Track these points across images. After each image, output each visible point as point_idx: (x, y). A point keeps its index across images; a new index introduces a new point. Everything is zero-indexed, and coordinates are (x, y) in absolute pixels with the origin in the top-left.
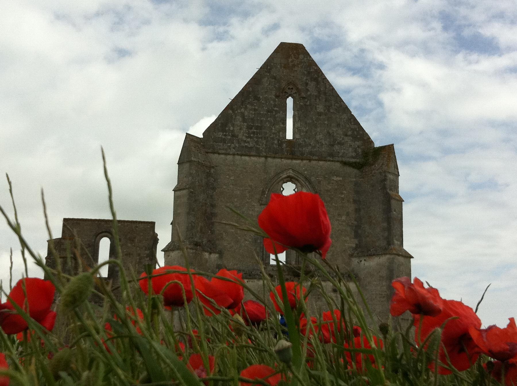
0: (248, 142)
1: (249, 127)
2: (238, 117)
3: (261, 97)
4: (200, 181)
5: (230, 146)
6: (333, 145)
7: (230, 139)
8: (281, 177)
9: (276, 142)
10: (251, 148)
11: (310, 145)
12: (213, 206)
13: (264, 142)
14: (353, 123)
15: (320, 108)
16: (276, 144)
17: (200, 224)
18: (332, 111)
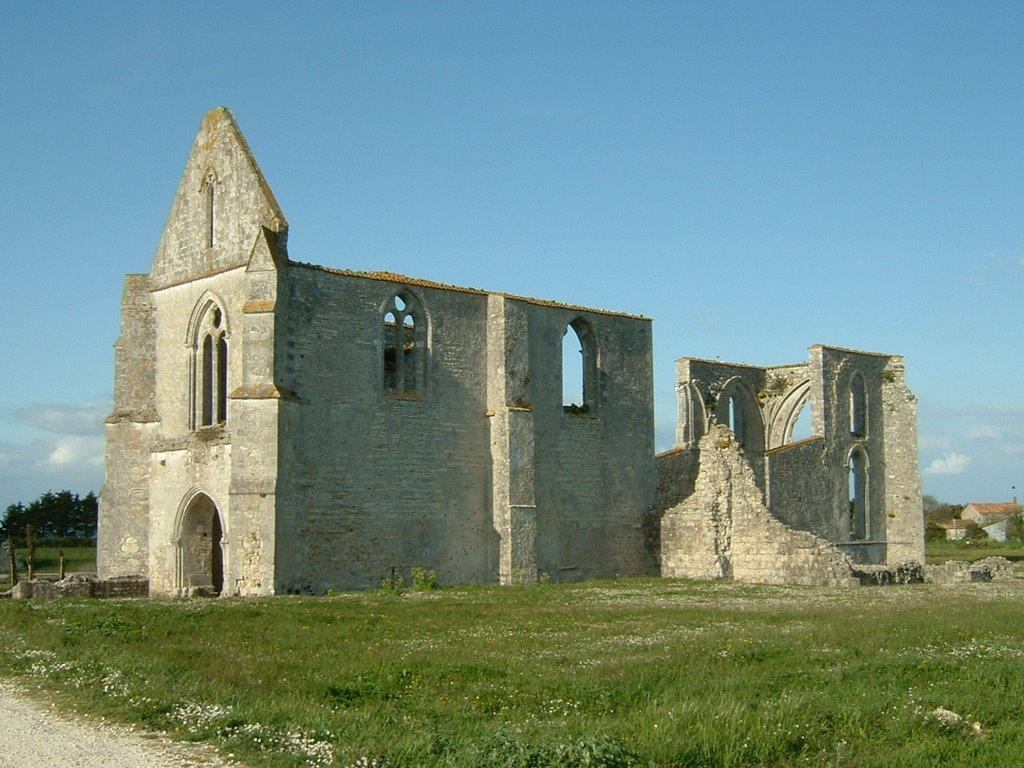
1: (181, 246)
12: (155, 359)
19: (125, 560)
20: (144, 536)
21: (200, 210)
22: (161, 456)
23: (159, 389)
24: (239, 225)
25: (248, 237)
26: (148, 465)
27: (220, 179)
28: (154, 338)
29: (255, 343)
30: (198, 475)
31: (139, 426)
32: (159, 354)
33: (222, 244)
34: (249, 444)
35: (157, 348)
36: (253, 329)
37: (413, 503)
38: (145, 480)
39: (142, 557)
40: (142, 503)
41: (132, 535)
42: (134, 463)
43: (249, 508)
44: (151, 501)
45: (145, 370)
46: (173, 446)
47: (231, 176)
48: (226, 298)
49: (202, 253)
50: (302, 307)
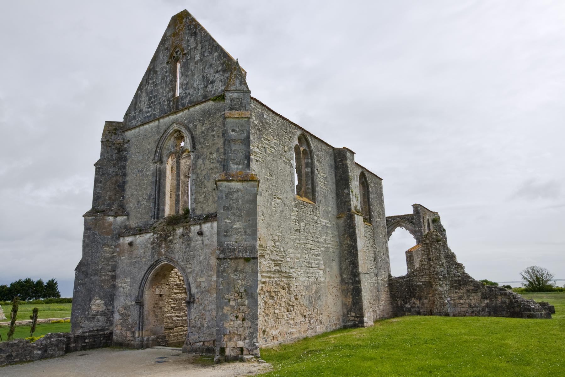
0: (149, 112)
2: (143, 94)
3: (158, 70)
4: (110, 157)
5: (138, 121)
6: (206, 87)
7: (138, 115)
8: (168, 133)
9: (166, 103)
10: (151, 115)
11: (189, 94)
12: (125, 175)
13: (159, 107)
14: (222, 58)
15: (197, 58)
16: (166, 105)
17: (109, 193)
18: (206, 55)
19: (93, 317)
20: (110, 298)
21: (167, 74)
22: (129, 239)
23: (128, 193)
24: (203, 76)
25: (212, 82)
26: (116, 247)
27: (185, 52)
28: (125, 161)
29: (235, 141)
30: (163, 251)
31: (111, 219)
32: (128, 171)
33: (187, 91)
34: (232, 218)
35: (127, 167)
36: (233, 131)
37: (311, 269)
38: (113, 257)
39: (108, 314)
40: (110, 274)
41: (101, 298)
42: (105, 245)
43: (236, 271)
44: (118, 272)
45: (116, 182)
46: (140, 231)
47: (195, 48)
48: (191, 126)
49: (168, 100)
50: (256, 127)
